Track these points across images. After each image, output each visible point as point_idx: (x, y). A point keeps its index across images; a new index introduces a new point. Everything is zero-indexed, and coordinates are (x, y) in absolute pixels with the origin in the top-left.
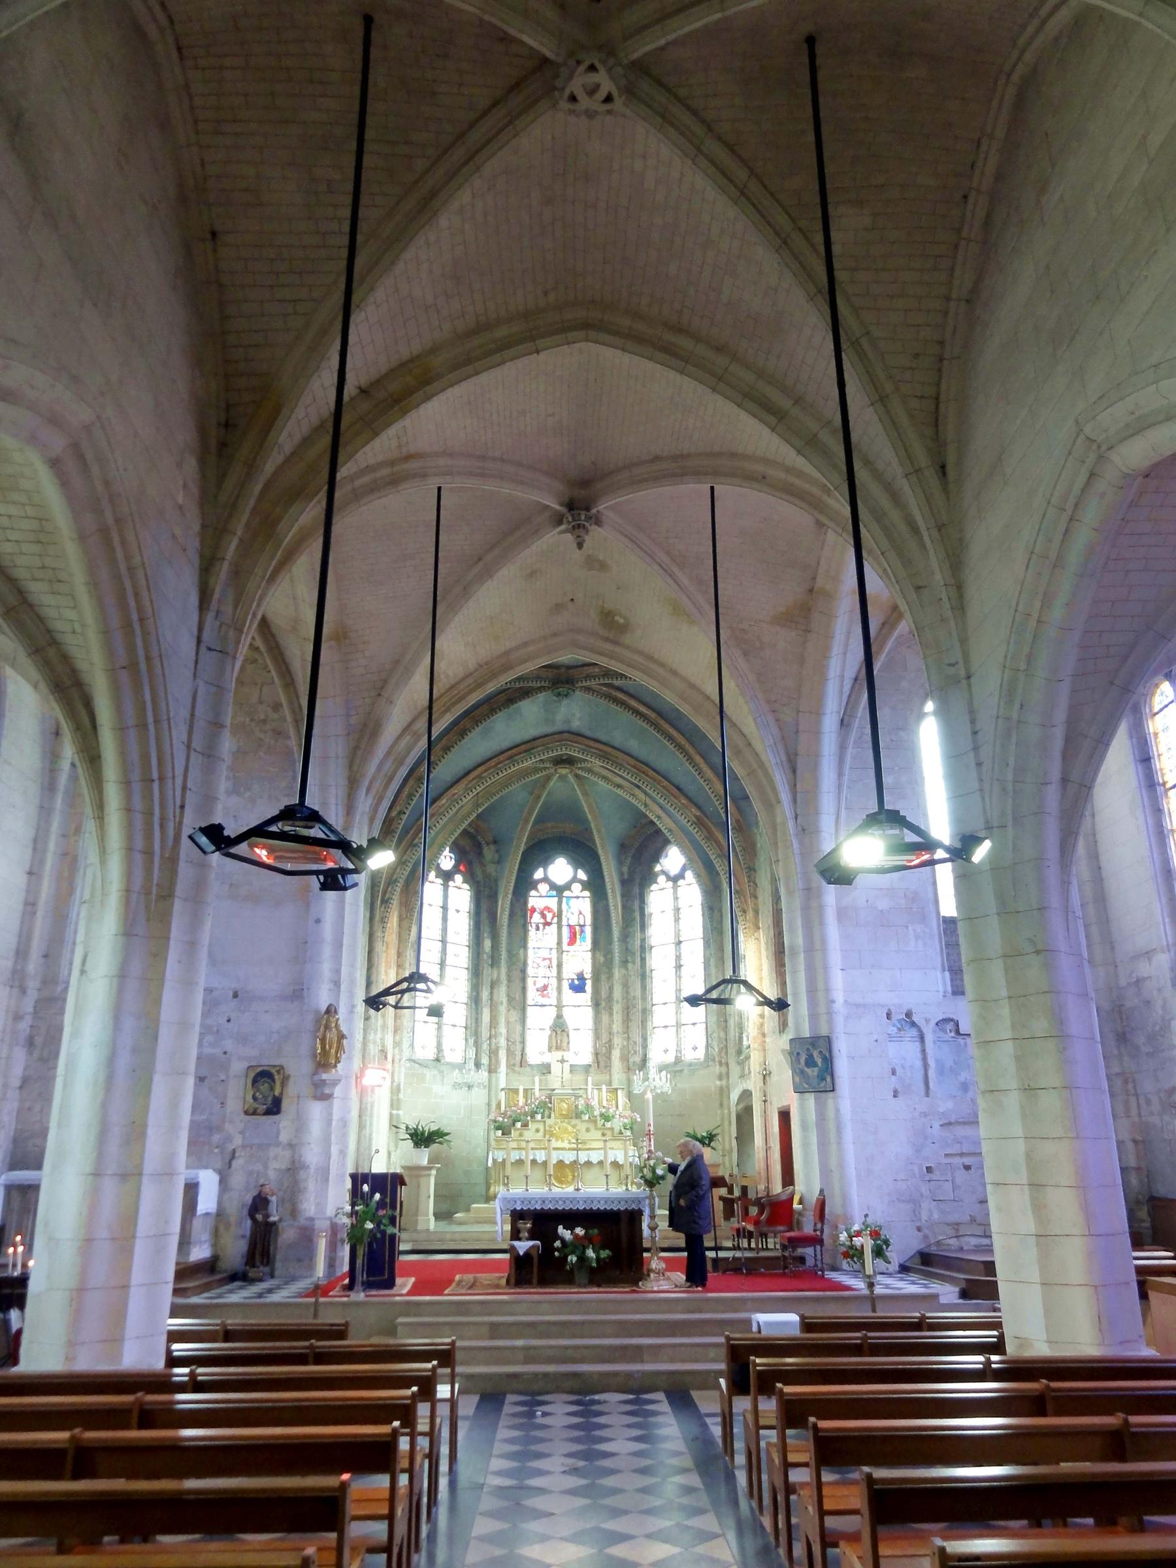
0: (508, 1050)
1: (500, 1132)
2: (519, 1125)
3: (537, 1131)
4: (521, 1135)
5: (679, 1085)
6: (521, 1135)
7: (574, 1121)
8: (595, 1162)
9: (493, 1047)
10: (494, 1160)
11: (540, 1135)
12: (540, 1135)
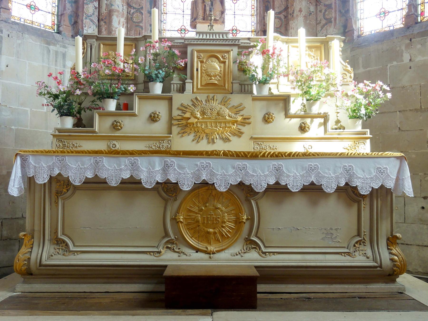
0: (129, 20)
1: (69, 122)
2: (112, 105)
3: (153, 118)
4: (115, 127)
5: (419, 59)
6: (115, 127)
7: (236, 99)
8: (295, 186)
9: (104, 10)
10: (30, 182)
11: (159, 128)
12: (159, 128)
